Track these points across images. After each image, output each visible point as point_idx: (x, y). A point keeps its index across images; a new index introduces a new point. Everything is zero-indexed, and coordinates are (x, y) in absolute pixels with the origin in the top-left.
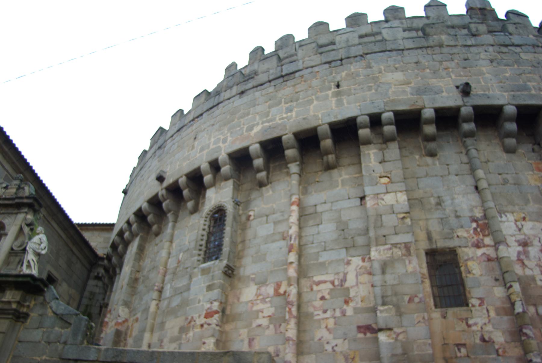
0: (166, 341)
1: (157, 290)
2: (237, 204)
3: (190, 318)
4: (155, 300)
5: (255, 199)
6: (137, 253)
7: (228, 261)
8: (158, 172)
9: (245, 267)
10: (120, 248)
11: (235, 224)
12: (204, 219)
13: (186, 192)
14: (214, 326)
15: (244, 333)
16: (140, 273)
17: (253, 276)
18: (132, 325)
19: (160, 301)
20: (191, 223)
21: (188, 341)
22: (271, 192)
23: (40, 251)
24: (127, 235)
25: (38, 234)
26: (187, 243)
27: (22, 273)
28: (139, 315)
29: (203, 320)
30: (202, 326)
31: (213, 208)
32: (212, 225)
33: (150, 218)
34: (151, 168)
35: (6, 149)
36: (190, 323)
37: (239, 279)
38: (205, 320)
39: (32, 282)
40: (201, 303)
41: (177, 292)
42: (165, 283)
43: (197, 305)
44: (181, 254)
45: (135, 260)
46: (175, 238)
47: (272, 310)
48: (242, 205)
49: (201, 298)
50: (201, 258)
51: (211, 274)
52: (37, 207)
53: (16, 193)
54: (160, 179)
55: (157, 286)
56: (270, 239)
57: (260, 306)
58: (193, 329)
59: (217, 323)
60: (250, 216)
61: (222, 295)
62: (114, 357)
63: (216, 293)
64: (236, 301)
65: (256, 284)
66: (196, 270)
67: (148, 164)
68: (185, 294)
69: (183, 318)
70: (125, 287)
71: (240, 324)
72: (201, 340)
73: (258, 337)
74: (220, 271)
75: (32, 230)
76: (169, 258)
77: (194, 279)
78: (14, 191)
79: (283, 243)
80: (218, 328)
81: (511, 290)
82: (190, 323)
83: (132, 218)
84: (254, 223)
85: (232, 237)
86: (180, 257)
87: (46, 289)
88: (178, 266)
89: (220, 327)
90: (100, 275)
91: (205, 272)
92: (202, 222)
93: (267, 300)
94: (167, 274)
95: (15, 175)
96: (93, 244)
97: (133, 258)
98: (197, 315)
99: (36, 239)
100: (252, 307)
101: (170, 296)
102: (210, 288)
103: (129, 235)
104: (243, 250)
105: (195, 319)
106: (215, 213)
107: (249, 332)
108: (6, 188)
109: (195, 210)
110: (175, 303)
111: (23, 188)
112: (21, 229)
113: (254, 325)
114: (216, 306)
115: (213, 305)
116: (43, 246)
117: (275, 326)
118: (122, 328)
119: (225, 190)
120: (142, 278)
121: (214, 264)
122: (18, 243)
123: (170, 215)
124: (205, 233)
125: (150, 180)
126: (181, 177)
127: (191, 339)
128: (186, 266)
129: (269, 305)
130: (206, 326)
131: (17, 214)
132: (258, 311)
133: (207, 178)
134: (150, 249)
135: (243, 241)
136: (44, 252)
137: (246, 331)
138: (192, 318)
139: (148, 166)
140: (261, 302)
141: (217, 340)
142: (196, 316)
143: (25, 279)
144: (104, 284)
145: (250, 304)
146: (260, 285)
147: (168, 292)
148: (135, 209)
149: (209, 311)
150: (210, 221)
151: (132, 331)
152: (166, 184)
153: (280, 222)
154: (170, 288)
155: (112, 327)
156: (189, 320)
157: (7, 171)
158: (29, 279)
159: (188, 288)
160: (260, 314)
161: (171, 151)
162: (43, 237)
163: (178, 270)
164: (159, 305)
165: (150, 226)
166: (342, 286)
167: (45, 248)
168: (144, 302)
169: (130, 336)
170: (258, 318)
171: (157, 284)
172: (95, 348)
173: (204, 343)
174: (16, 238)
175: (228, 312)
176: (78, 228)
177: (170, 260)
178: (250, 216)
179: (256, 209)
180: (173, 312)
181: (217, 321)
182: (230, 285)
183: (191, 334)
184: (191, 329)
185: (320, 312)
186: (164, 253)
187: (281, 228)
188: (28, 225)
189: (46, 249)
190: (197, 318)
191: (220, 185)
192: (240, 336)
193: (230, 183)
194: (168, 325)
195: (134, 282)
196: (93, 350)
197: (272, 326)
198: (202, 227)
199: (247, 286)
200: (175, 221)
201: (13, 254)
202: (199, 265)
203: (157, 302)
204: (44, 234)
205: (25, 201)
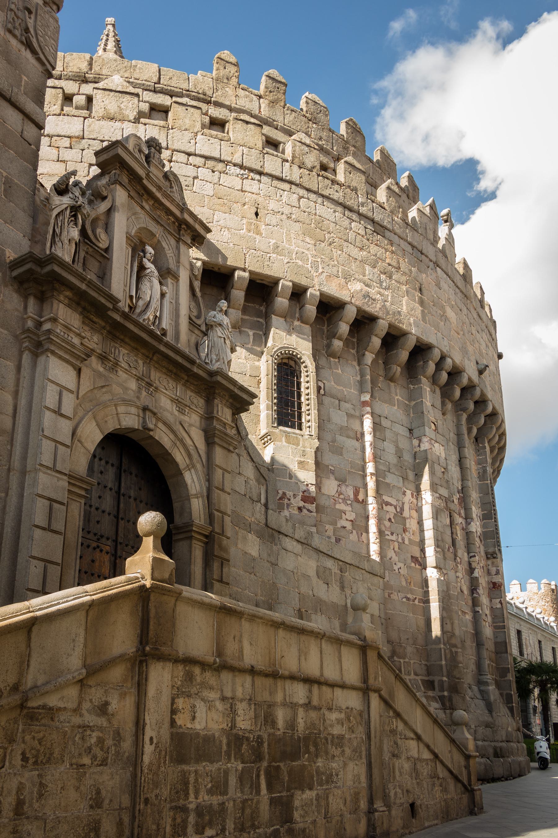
3: (280, 492)
30: (300, 509)
58: (288, 508)
65: (336, 479)
73: (344, 539)
81: (472, 559)
98: (291, 494)
100: (335, 504)
117: (357, 533)
126: (244, 270)
130: (305, 511)
138: (284, 494)
142: (289, 494)
160: (343, 514)
166: (401, 514)
185: (389, 533)
197: (354, 532)
199: (328, 478)
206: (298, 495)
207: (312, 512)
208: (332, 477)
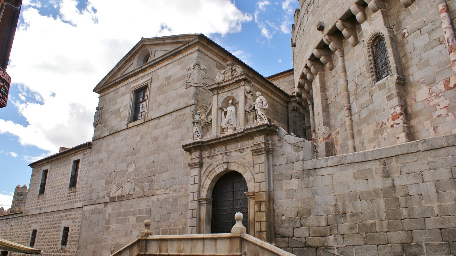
0: (366, 143)
1: (347, 109)
2: (390, 28)
4: (348, 116)
5: (404, 19)
6: (321, 87)
7: (398, 74)
8: (317, 22)
9: (413, 75)
10: (306, 87)
11: (393, 44)
12: (366, 48)
13: (345, 32)
14: (401, 124)
15: (427, 124)
16: (328, 100)
17: (423, 80)
18: (336, 137)
19: (352, 116)
20: (356, 54)
21: (385, 139)
22: (417, 9)
23: (264, 107)
24: (308, 76)
25: (258, 97)
26: (358, 69)
27: (259, 125)
28: (338, 129)
29: (392, 122)
30: (392, 126)
31: (371, 37)
32: (374, 50)
33: (322, 59)
34: (309, 22)
35: (210, 47)
36: (381, 126)
37: (411, 85)
38: (393, 121)
39: (268, 128)
40: (386, 111)
41: (363, 107)
42: (351, 103)
43: (383, 112)
44: (356, 79)
45: (321, 92)
46: (347, 68)
47: (447, 101)
48: (394, 27)
49: (385, 107)
50: (374, 78)
51: (387, 87)
52: (249, 79)
53: (232, 75)
54: (321, 28)
55: (346, 106)
56: (427, 48)
57: (436, 101)
59: (404, 122)
60: (405, 33)
61: (401, 101)
62: (338, 162)
63: (396, 101)
64: (413, 102)
65: (427, 85)
66: (374, 87)
67: (305, 19)
68: (370, 107)
69: (375, 124)
70: (321, 113)
71: (422, 118)
72: (395, 136)
73: (440, 125)
74: (394, 84)
75: (252, 95)
76: (348, 84)
77: (375, 95)
78: (230, 73)
79: (441, 47)
80: (405, 125)
82: (381, 126)
83: (309, 64)
84: (410, 39)
85: (394, 55)
86: (357, 81)
87: (277, 130)
88: (357, 88)
89: (407, 124)
90: (295, 108)
91: (380, 87)
92: (366, 50)
93: (440, 95)
94: (350, 95)
95: (224, 64)
96: (282, 88)
97: (319, 91)
99: (258, 100)
100: (429, 103)
101: (358, 111)
102: (389, 98)
103: (310, 76)
104: (407, 62)
105: (385, 123)
106: (374, 41)
107: (431, 123)
108: (225, 73)
109: (356, 42)
110: (364, 114)
111: (235, 70)
112: (245, 96)
113: (434, 116)
114: (398, 110)
115: (396, 110)
116: (264, 103)
118: (329, 141)
119: (376, 20)
120: (331, 103)
121: (387, 79)
122: (248, 106)
123: (337, 53)
124: (371, 58)
125: (312, 31)
127: (386, 137)
128: (363, 87)
129: (443, 98)
130: (395, 126)
131: (238, 88)
132: (435, 106)
133: (359, 16)
134: (330, 82)
135: (405, 55)
136: (267, 107)
137: (429, 121)
138: (383, 122)
139: (305, 21)
140: (435, 98)
141: (407, 134)
142: (385, 121)
143: (263, 128)
144: (300, 113)
145: (426, 102)
146: (431, 85)
147: (355, 108)
148: (308, 56)
149: (394, 114)
150: (372, 47)
151: (337, 141)
152: (326, 31)
153: (433, 30)
154: (356, 105)
155: (321, 141)
156: (380, 125)
157: (217, 62)
158: (266, 127)
159: (371, 101)
160: (437, 106)
161: (320, 5)
162: (262, 97)
163: (358, 90)
164: (353, 119)
165: (323, 65)
167: (266, 104)
168: (339, 119)
169: (337, 145)
170: (436, 110)
171: (345, 105)
172: (324, 159)
173: (398, 138)
174: (246, 103)
175: (409, 111)
176: (268, 79)
177: (348, 85)
178: (405, 33)
179: (408, 26)
180: (365, 121)
181: (403, 120)
182: (404, 92)
183: (385, 134)
184: (384, 130)
186: (342, 82)
187: (436, 35)
188: (249, 93)
189: (267, 105)
190: (387, 121)
191: (371, 18)
192: (425, 127)
193: (379, 12)
194: (363, 132)
195: (326, 108)
196: (323, 160)
197: (450, 114)
198: (367, 54)
200: (343, 56)
201: (247, 114)
202: (375, 83)
203: (350, 117)
204: (262, 95)
205: (240, 78)
206: (390, 118)
207: (399, 124)
208: (423, 86)
